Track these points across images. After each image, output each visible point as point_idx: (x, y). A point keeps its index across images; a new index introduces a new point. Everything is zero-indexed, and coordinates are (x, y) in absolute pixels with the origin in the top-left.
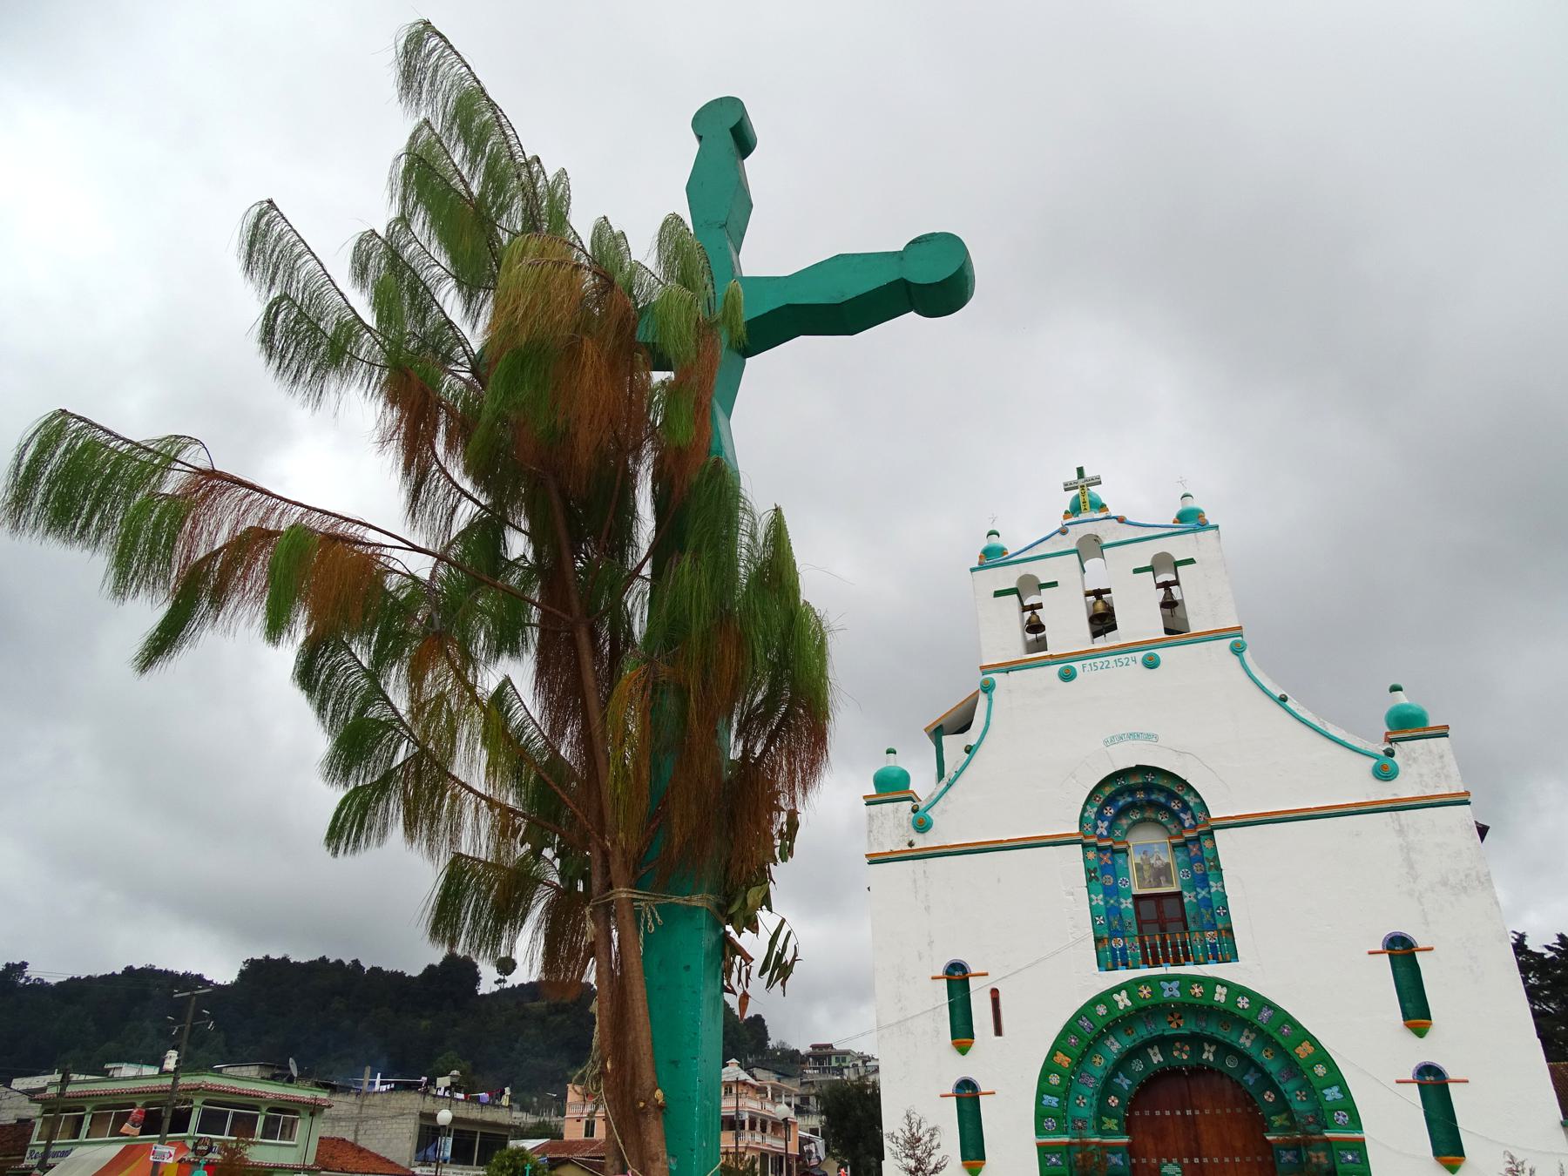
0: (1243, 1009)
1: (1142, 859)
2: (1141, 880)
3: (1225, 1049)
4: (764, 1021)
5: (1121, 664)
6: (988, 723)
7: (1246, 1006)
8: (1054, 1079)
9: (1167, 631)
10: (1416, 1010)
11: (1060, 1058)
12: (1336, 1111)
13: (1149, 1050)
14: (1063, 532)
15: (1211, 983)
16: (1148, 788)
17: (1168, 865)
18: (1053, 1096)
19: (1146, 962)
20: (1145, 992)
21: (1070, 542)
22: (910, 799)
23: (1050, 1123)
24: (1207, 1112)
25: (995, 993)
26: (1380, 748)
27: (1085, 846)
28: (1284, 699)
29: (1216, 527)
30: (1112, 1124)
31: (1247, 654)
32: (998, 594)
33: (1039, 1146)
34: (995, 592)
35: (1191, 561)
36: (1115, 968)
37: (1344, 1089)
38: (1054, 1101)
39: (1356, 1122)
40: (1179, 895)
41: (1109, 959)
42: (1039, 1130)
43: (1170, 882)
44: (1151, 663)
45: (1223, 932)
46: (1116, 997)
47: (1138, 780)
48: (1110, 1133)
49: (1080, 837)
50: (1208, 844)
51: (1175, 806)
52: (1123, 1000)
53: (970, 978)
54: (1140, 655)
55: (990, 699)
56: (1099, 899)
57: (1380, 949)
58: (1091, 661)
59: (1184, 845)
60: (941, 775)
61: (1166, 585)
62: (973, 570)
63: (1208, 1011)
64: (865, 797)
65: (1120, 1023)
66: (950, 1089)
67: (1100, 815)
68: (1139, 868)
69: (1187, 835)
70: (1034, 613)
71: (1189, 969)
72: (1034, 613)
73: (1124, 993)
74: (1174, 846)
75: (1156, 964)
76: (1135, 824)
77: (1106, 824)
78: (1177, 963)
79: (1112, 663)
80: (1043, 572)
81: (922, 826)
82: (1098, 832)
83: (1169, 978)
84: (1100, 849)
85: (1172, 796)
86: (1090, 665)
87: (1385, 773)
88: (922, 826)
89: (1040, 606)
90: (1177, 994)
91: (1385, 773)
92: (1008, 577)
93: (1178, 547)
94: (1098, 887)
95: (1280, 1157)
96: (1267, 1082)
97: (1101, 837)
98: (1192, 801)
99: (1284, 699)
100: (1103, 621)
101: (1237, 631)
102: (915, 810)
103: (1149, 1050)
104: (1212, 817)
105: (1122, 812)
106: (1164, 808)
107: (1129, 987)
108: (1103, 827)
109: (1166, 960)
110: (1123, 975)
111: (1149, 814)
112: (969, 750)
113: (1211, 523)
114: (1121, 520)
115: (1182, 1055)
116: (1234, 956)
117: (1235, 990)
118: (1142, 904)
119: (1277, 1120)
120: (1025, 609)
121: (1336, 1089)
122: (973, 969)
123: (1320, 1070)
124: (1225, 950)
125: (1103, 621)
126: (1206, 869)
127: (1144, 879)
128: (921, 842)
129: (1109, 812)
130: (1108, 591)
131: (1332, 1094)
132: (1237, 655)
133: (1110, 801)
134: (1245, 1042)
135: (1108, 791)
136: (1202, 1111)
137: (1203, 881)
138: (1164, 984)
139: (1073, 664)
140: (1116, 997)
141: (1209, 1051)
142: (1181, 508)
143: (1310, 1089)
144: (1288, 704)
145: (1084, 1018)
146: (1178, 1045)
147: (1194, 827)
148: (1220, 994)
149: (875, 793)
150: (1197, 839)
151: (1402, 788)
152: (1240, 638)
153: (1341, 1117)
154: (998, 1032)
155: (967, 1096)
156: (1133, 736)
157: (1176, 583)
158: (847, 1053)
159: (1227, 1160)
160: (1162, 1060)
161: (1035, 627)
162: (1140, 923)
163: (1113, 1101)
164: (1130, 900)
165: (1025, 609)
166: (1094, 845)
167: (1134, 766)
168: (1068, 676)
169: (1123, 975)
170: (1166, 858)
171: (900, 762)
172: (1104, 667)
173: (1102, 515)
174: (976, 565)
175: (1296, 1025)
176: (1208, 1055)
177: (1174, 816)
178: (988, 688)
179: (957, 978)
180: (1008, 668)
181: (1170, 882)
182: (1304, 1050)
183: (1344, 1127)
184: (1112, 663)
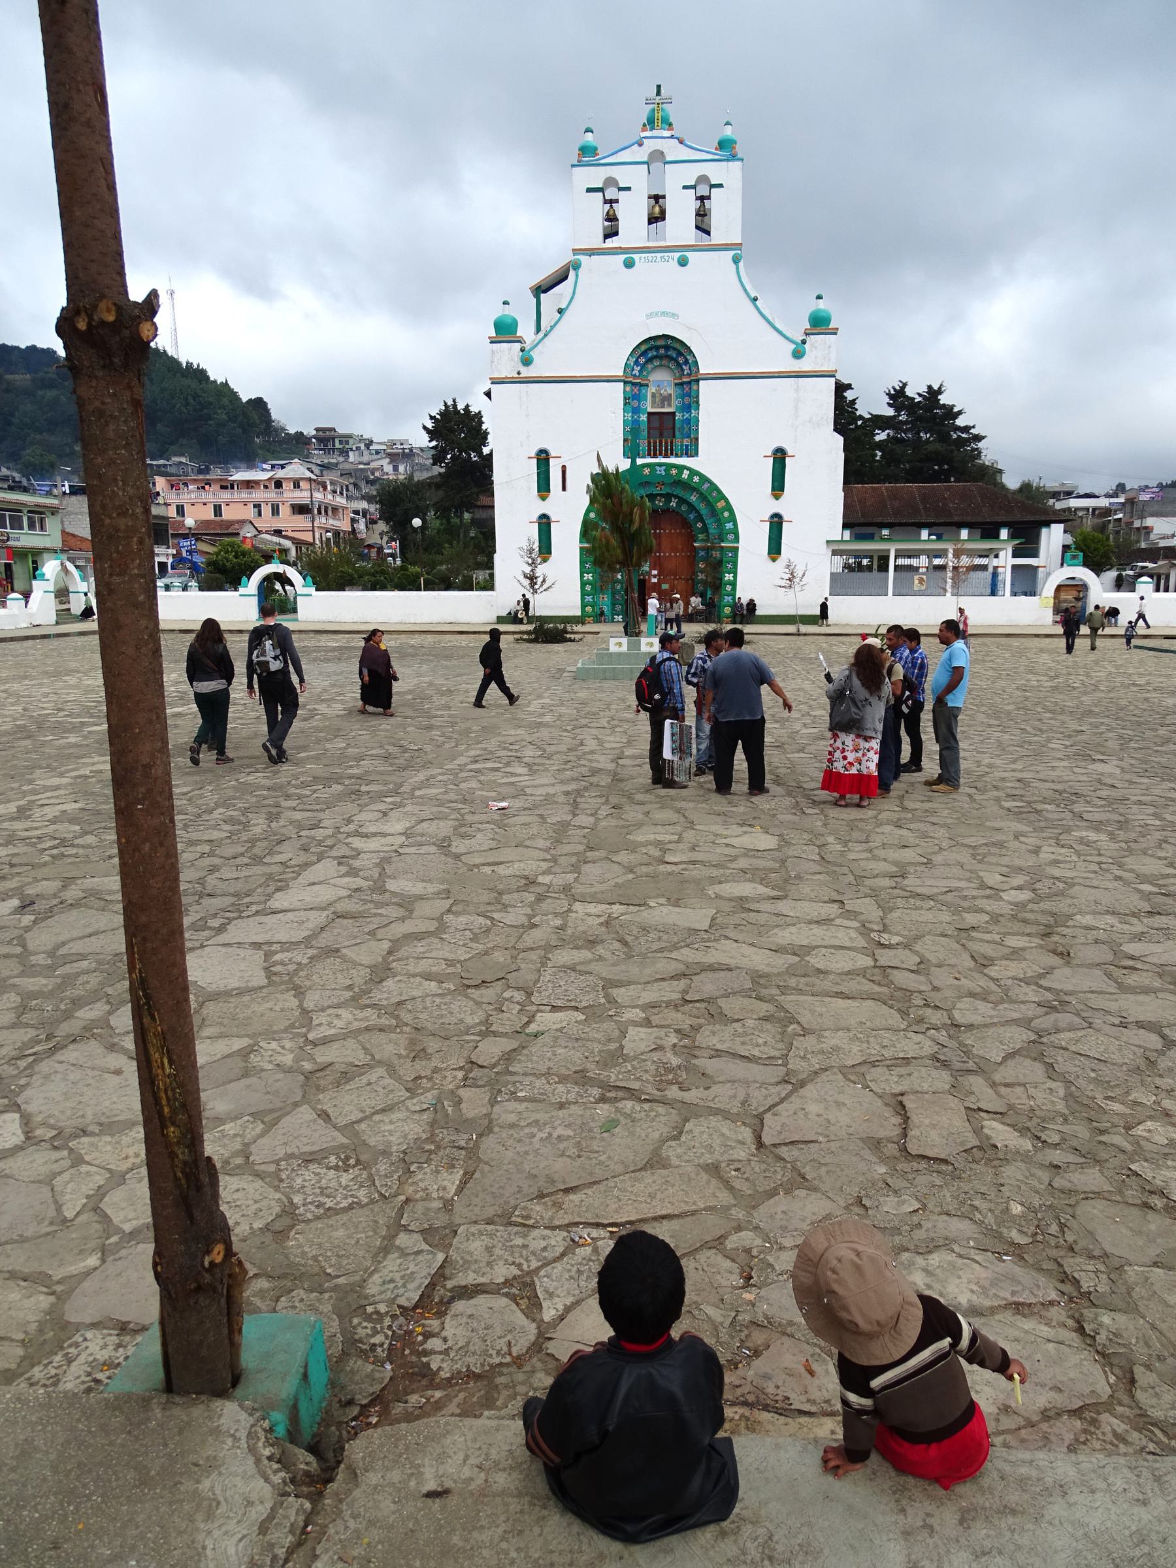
2: (653, 402)
3: (682, 501)
4: (265, 404)
10: (778, 486)
15: (681, 468)
16: (667, 348)
17: (670, 395)
19: (649, 454)
21: (642, 154)
22: (519, 342)
25: (564, 469)
26: (799, 337)
27: (625, 383)
28: (755, 299)
31: (741, 264)
32: (589, 190)
35: (720, 186)
37: (735, 525)
39: (737, 539)
40: (673, 414)
43: (669, 405)
44: (683, 262)
50: (694, 387)
51: (681, 360)
54: (677, 255)
59: (682, 384)
60: (538, 329)
61: (702, 199)
63: (678, 483)
67: (636, 363)
68: (653, 395)
71: (672, 460)
74: (676, 384)
75: (655, 456)
78: (666, 456)
80: (623, 176)
81: (527, 362)
83: (660, 465)
84: (634, 384)
85: (680, 354)
87: (798, 354)
88: (527, 362)
89: (617, 201)
91: (798, 354)
92: (596, 176)
93: (715, 172)
94: (629, 408)
96: (700, 518)
99: (755, 299)
101: (738, 246)
102: (522, 350)
105: (650, 360)
111: (664, 362)
113: (739, 156)
117: (694, 473)
118: (652, 417)
119: (701, 536)
120: (606, 202)
122: (553, 454)
123: (726, 514)
126: (691, 402)
128: (526, 372)
129: (642, 360)
130: (664, 197)
131: (729, 526)
133: (644, 354)
134: (693, 498)
135: (643, 348)
137: (687, 408)
143: (720, 523)
144: (757, 303)
147: (689, 375)
148: (685, 475)
150: (690, 383)
151: (804, 365)
153: (731, 537)
154: (564, 489)
155: (544, 523)
156: (664, 314)
157: (709, 198)
158: (350, 436)
161: (611, 218)
162: (649, 428)
168: (629, 264)
170: (670, 390)
173: (667, 133)
175: (719, 492)
177: (679, 365)
178: (577, 266)
179: (543, 458)
180: (591, 252)
181: (669, 405)
182: (721, 505)
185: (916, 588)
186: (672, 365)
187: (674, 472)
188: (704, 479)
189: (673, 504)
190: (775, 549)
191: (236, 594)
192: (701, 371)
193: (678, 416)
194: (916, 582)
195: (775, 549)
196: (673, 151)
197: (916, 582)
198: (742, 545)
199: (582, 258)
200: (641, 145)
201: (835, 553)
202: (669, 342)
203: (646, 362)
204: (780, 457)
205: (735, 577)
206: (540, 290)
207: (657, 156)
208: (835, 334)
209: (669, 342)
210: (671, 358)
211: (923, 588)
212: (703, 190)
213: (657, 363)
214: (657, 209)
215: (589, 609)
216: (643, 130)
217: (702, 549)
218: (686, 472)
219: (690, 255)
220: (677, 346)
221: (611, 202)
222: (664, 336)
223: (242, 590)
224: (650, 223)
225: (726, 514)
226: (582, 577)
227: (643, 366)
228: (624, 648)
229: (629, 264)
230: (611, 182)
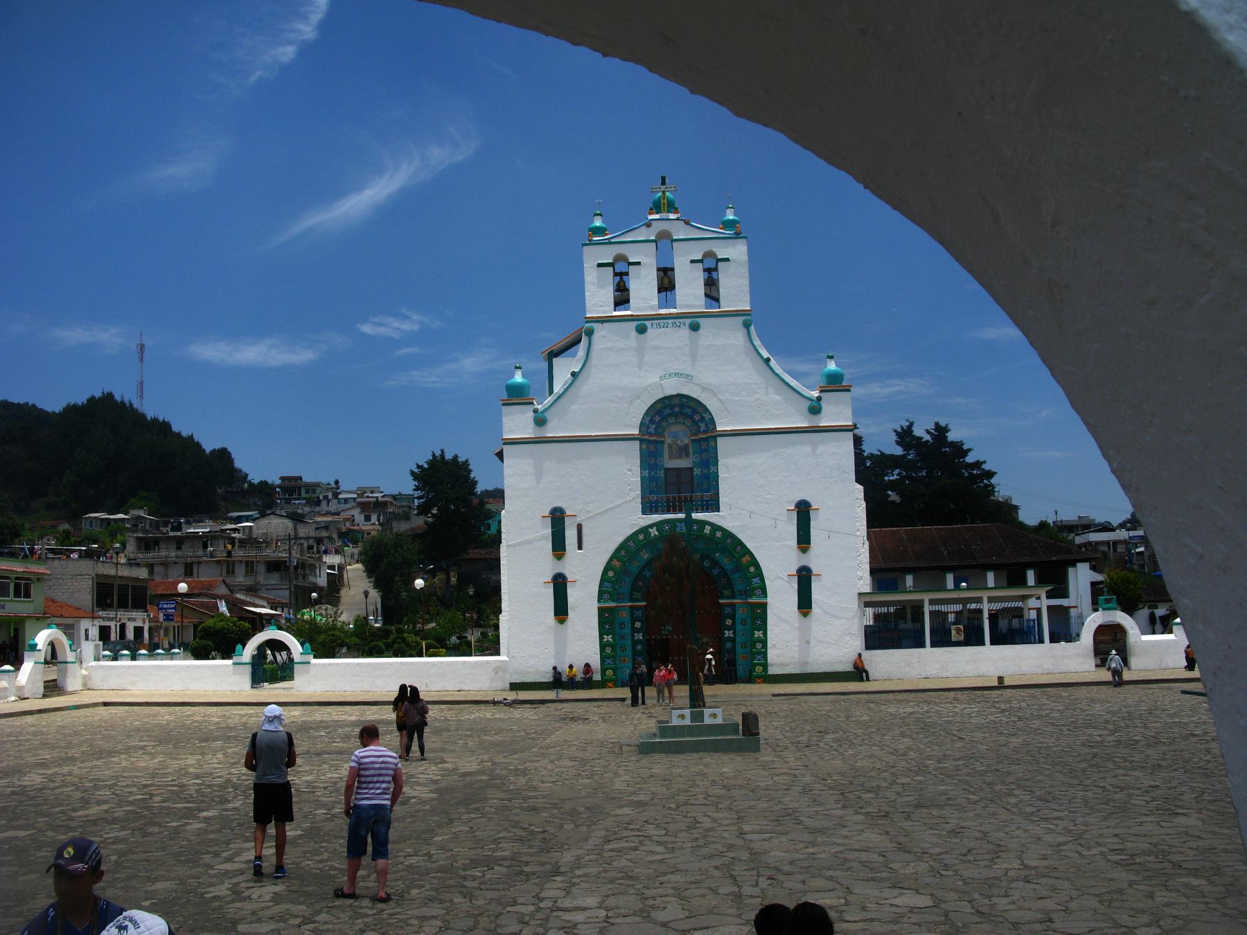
8: (611, 574)
10: (804, 540)
11: (616, 563)
15: (703, 523)
16: (682, 406)
25: (580, 528)
27: (641, 441)
28: (768, 360)
30: (638, 595)
31: (752, 328)
36: (651, 513)
40: (691, 470)
41: (648, 508)
46: (650, 530)
47: (677, 401)
48: (638, 600)
50: (712, 443)
51: (697, 417)
52: (654, 532)
54: (688, 321)
56: (646, 473)
57: (793, 508)
58: (657, 322)
64: (502, 400)
66: (550, 580)
67: (652, 421)
70: (621, 278)
72: (621, 278)
73: (655, 528)
77: (654, 426)
79: (670, 325)
82: (649, 431)
85: (695, 412)
88: (540, 421)
91: (815, 410)
92: (607, 255)
95: (724, 610)
97: (651, 434)
98: (706, 416)
99: (768, 360)
104: (718, 429)
105: (664, 418)
106: (691, 417)
107: (658, 525)
108: (652, 429)
110: (656, 518)
116: (717, 509)
117: (716, 527)
119: (726, 593)
120: (616, 274)
122: (568, 513)
123: (752, 569)
124: (713, 505)
126: (709, 460)
129: (657, 418)
133: (659, 412)
139: (645, 322)
140: (650, 530)
147: (705, 432)
150: (706, 439)
154: (580, 547)
164: (663, 472)
167: (675, 393)
169: (656, 518)
178: (590, 333)
179: (557, 518)
182: (745, 560)
183: (759, 596)
184: (670, 325)
185: (954, 639)
188: (728, 535)
190: (805, 603)
191: (229, 662)
192: (718, 429)
193: (697, 472)
194: (954, 632)
195: (805, 603)
196: (680, 232)
198: (769, 600)
201: (867, 605)
203: (661, 421)
204: (803, 511)
205: (765, 634)
207: (664, 236)
208: (849, 391)
209: (684, 400)
210: (686, 416)
211: (962, 638)
212: (710, 263)
213: (671, 420)
214: (666, 281)
215: (609, 673)
216: (650, 214)
218: (708, 528)
219: (701, 321)
223: (236, 659)
224: (659, 291)
225: (752, 569)
227: (658, 426)
228: (687, 722)
229: (642, 330)
230: (620, 258)
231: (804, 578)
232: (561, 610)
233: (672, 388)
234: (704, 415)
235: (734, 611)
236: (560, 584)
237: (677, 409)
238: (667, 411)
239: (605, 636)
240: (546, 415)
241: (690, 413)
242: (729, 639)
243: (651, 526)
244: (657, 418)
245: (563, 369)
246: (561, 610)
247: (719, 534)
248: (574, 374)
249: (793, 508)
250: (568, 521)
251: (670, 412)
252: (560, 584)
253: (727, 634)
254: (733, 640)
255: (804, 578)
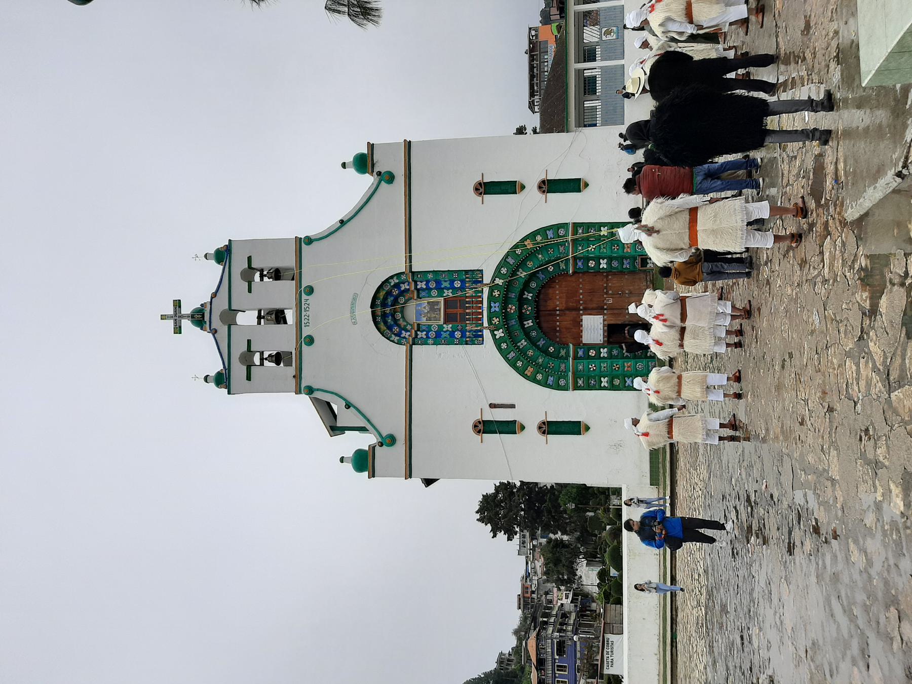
0: (507, 271)
1: (424, 317)
5: (308, 308)
6: (332, 393)
7: (506, 269)
9: (293, 279)
10: (510, 188)
12: (558, 234)
13: (526, 327)
14: (214, 332)
17: (428, 303)
18: (548, 379)
20: (496, 321)
21: (223, 330)
22: (374, 448)
23: (562, 382)
24: (558, 303)
25: (492, 406)
29: (230, 240)
30: (563, 353)
33: (574, 389)
34: (247, 379)
35: (249, 259)
36: (482, 336)
38: (551, 379)
39: (564, 225)
40: (446, 301)
41: (476, 338)
42: (565, 388)
44: (310, 290)
45: (467, 276)
49: (409, 345)
51: (396, 292)
52: (499, 334)
53: (483, 419)
54: (304, 297)
55: (318, 390)
60: (362, 429)
61: (262, 276)
62: (229, 393)
65: (511, 336)
66: (543, 438)
67: (398, 335)
68: (429, 319)
69: (413, 288)
70: (266, 359)
73: (496, 332)
74: (419, 297)
76: (403, 317)
77: (403, 332)
80: (239, 348)
81: (391, 440)
83: (490, 307)
85: (389, 293)
86: (305, 326)
87: (390, 178)
88: (391, 440)
90: (497, 304)
91: (390, 178)
92: (238, 370)
93: (239, 264)
100: (279, 317)
102: (381, 444)
103: (526, 327)
105: (396, 321)
106: (396, 299)
109: (480, 308)
110: (487, 334)
112: (348, 406)
114: (214, 295)
115: (528, 310)
117: (497, 273)
121: (548, 232)
122: (479, 417)
123: (539, 238)
125: (279, 317)
127: (435, 317)
129: (396, 329)
132: (312, 242)
133: (390, 328)
134: (523, 274)
136: (557, 306)
138: (493, 310)
141: (527, 295)
142: (214, 261)
145: (508, 356)
146: (523, 311)
149: (367, 472)
152: (302, 240)
157: (262, 271)
159: (581, 297)
160: (531, 321)
163: (551, 349)
165: (262, 364)
166: (414, 339)
168: (310, 340)
169: (487, 334)
170: (425, 302)
171: (349, 453)
172: (308, 318)
174: (226, 390)
175: (516, 246)
176: (529, 296)
177: (402, 293)
179: (485, 427)
180: (298, 377)
181: (437, 303)
182: (529, 244)
183: (567, 231)
186: (402, 300)
187: (496, 293)
188: (504, 262)
189: (529, 296)
194: (609, 37)
196: (221, 304)
197: (609, 37)
199: (303, 385)
200: (216, 331)
202: (378, 302)
204: (486, 188)
206: (335, 429)
209: (378, 302)
213: (399, 315)
217: (575, 264)
220: (382, 294)
221: (262, 359)
222: (372, 307)
226: (605, 388)
231: (550, 186)
232: (574, 428)
233: (365, 312)
234: (392, 284)
235: (580, 258)
236: (550, 428)
237: (388, 310)
238: (390, 320)
239: (602, 385)
240: (384, 434)
241: (392, 298)
242: (609, 263)
243: (494, 336)
244: (396, 329)
245: (345, 418)
246: (574, 428)
247: (504, 271)
248: (348, 406)
249: (481, 198)
250: (487, 417)
251: (390, 317)
252: (550, 428)
253: (603, 264)
254: (610, 259)
255: (550, 186)
